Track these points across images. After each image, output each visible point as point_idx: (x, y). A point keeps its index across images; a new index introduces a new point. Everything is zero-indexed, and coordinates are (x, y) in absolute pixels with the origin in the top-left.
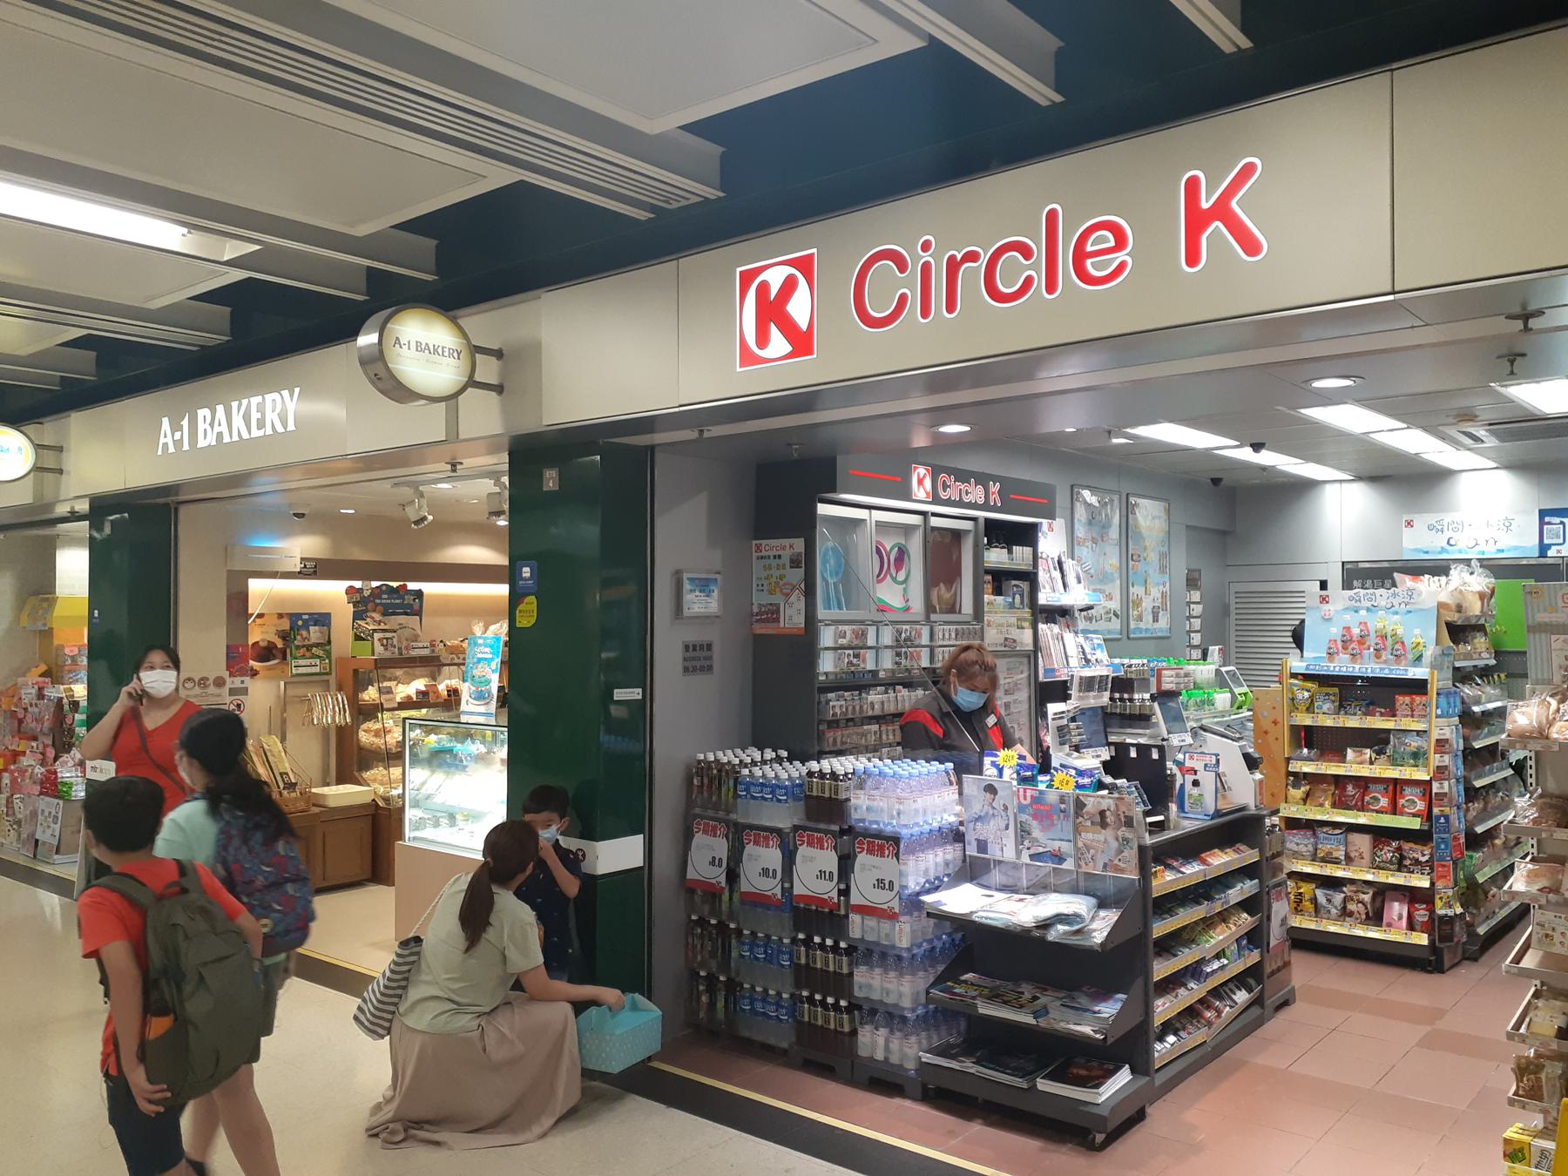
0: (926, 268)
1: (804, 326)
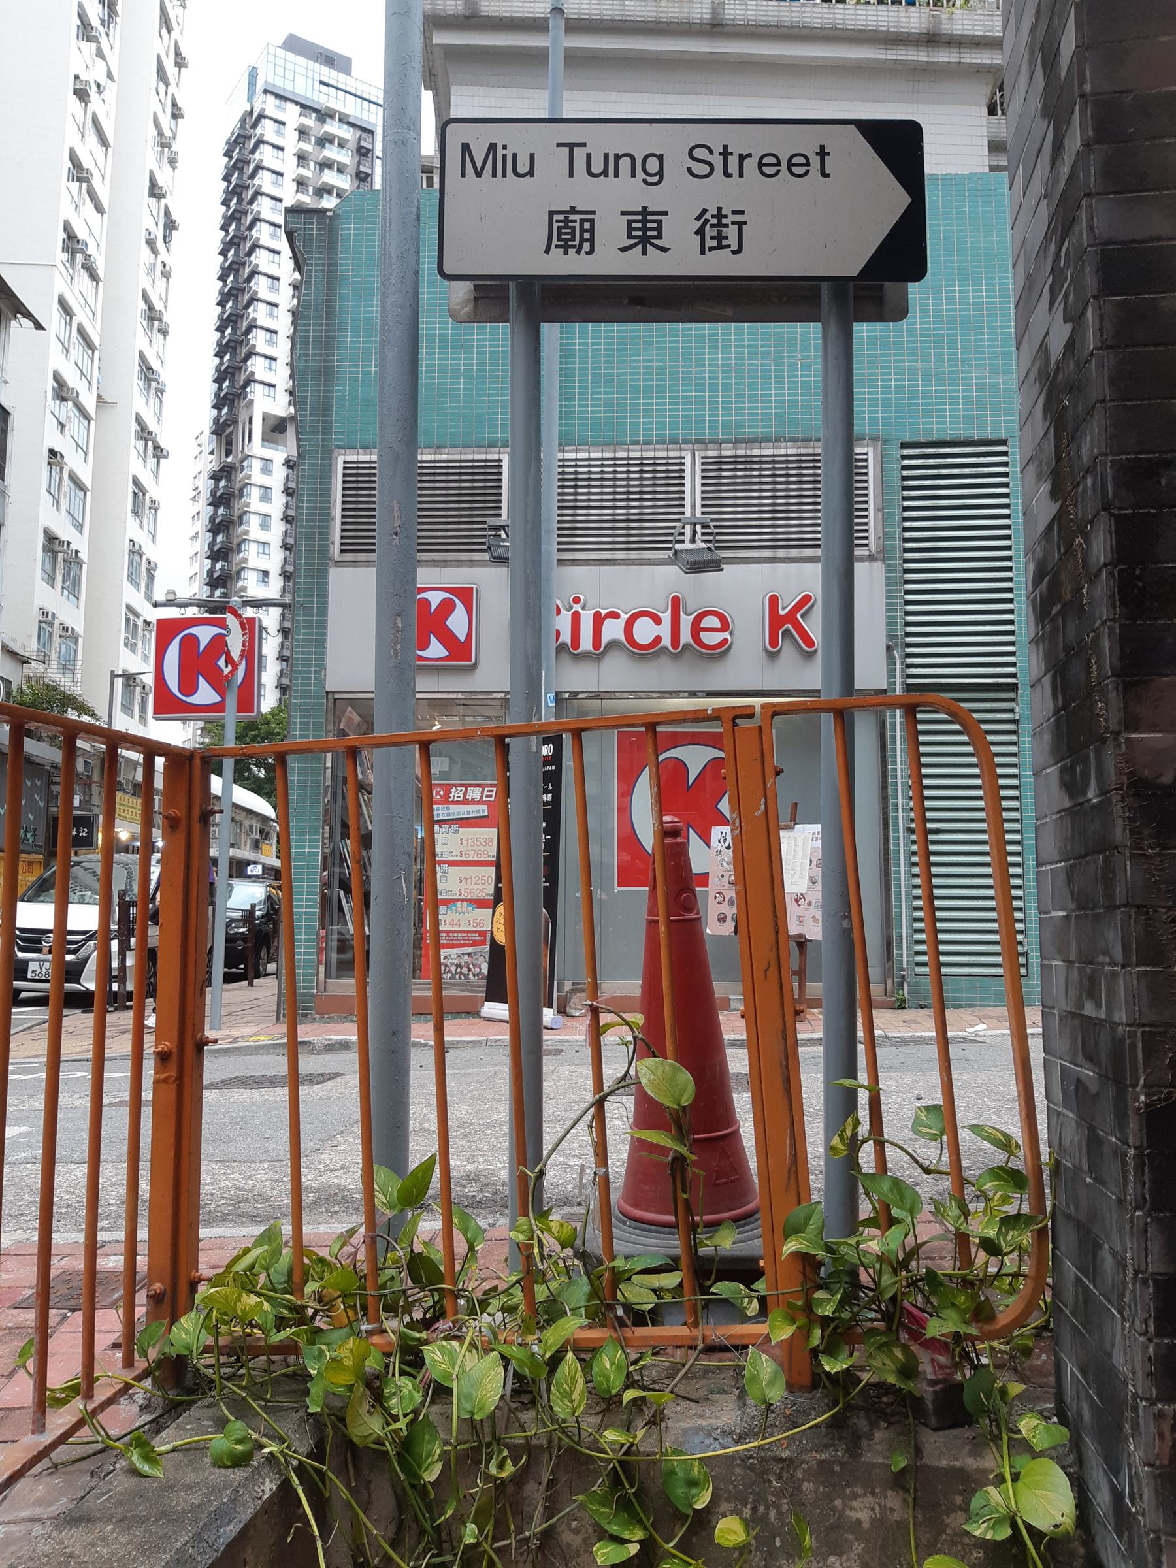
0: (576, 617)
1: (462, 640)
